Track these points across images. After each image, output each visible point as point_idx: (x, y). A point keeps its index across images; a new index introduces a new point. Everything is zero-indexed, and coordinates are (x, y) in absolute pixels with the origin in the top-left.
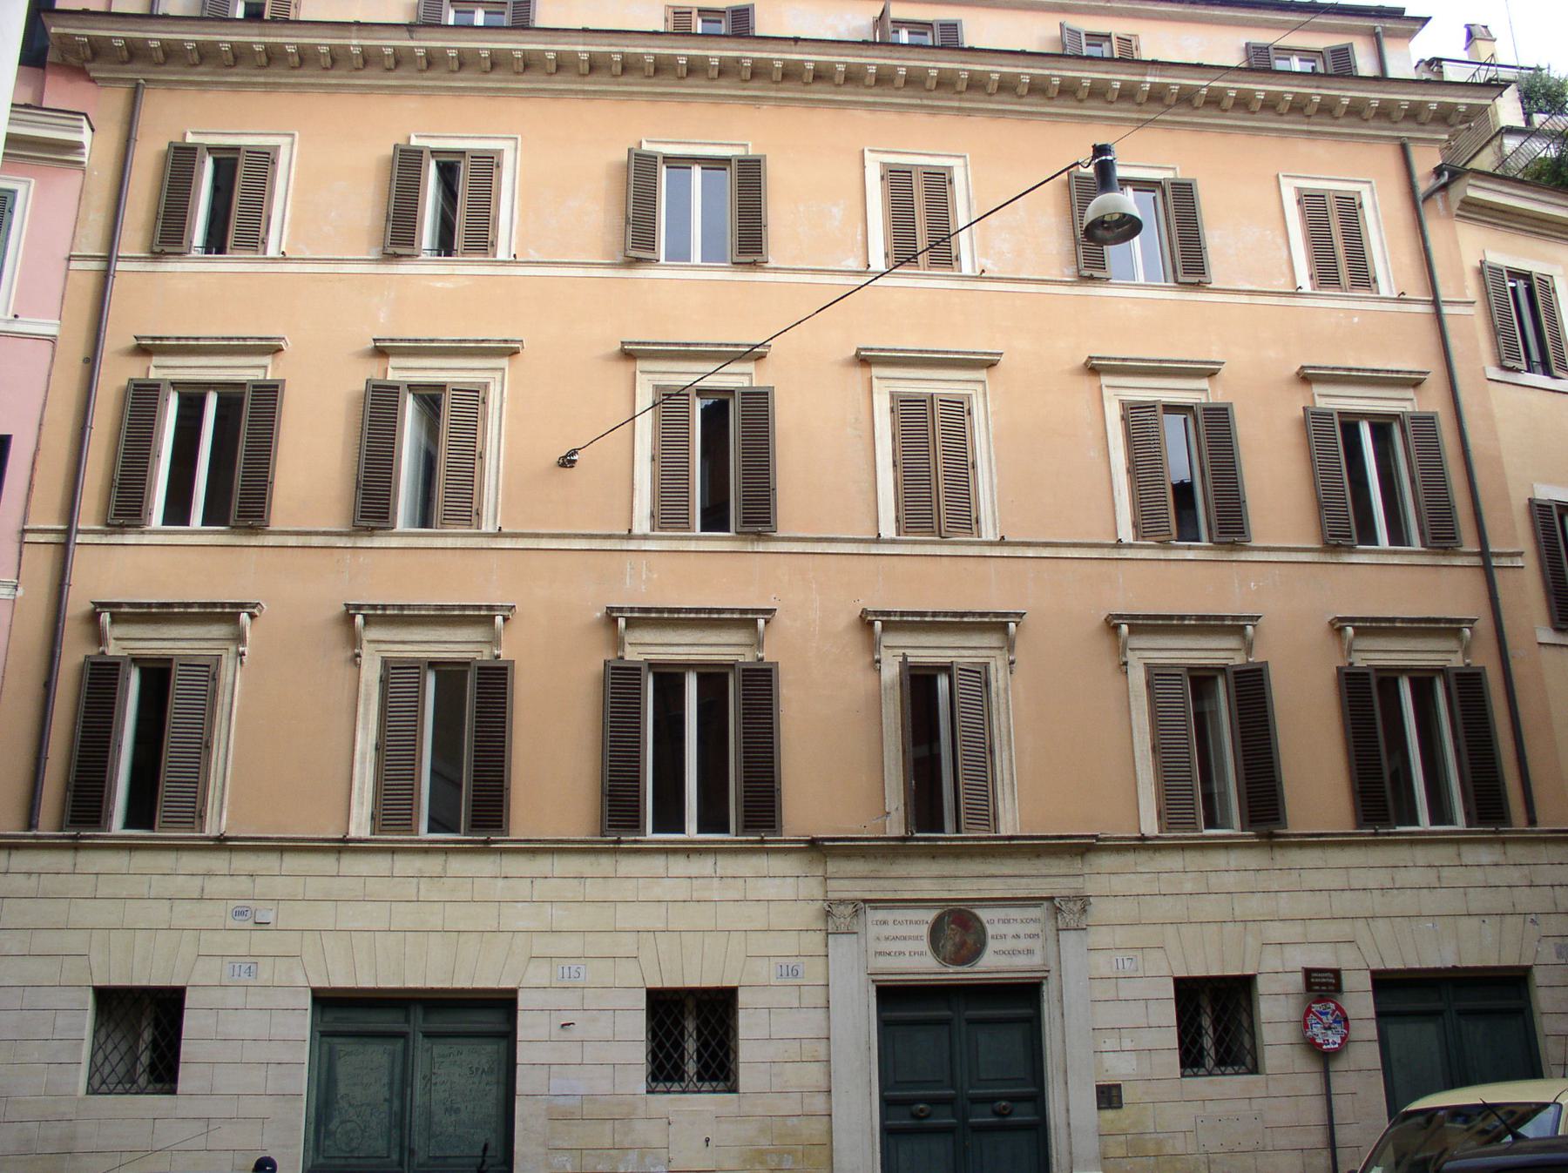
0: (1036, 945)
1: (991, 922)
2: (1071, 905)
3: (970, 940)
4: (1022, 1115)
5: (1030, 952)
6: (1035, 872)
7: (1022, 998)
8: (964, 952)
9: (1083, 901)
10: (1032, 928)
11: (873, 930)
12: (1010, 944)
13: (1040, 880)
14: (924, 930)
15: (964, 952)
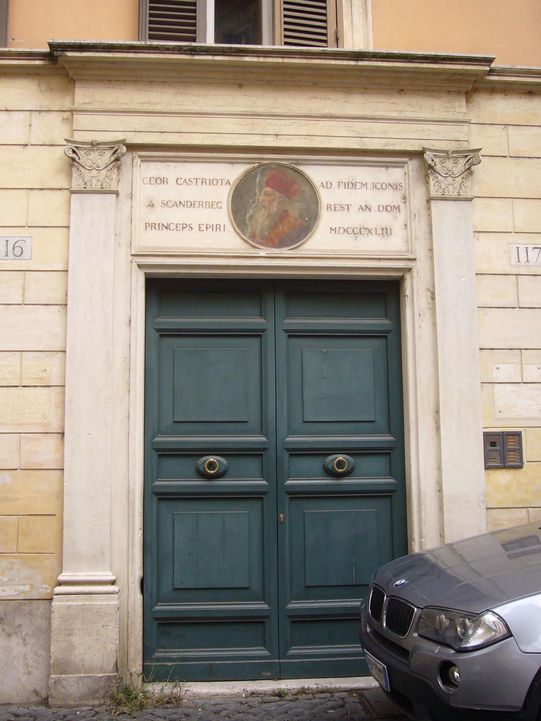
0: (396, 222)
1: (328, 185)
2: (449, 164)
3: (295, 209)
4: (370, 476)
5: (386, 232)
6: (395, 115)
7: (375, 296)
8: (284, 228)
9: (470, 157)
10: (390, 197)
11: (144, 192)
13: (401, 126)
14: (224, 194)
15: (284, 228)
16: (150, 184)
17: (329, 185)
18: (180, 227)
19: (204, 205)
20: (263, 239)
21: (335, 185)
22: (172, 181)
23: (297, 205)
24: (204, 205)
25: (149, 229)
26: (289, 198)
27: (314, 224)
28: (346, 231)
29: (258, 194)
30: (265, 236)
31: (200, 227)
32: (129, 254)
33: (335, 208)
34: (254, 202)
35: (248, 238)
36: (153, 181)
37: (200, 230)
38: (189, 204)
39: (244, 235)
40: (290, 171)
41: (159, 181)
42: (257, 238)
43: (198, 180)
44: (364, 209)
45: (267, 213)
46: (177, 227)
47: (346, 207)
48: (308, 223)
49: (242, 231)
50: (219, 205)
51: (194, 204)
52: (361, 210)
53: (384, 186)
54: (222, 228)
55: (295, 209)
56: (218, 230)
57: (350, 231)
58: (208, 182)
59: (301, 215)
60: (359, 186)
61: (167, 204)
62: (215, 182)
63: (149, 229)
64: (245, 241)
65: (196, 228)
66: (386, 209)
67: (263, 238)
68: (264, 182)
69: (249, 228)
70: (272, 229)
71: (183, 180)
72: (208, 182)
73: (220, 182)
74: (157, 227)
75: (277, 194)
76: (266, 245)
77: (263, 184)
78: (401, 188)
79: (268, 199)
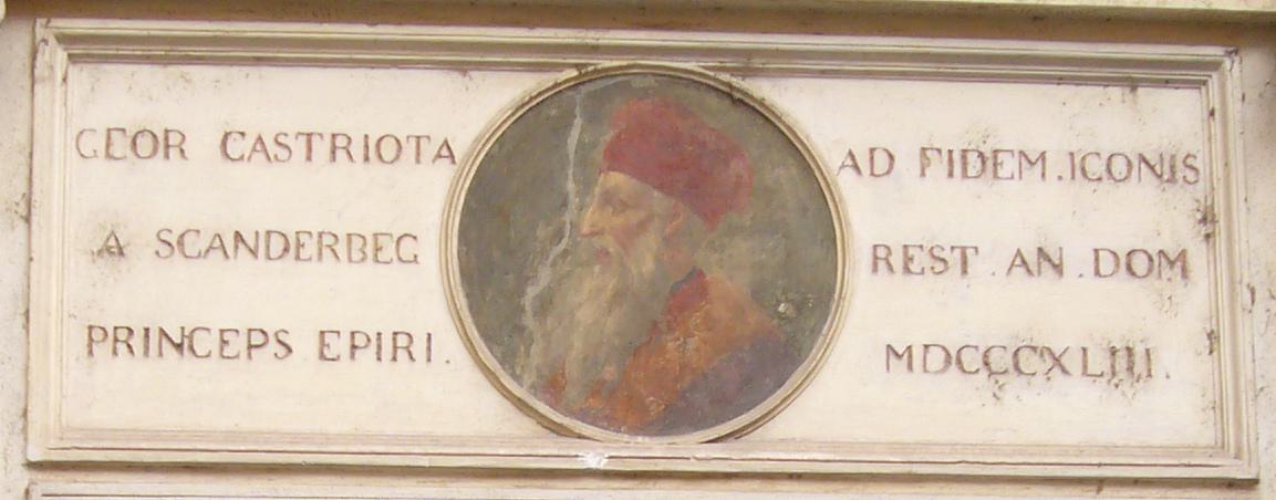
1: (877, 163)
3: (733, 266)
5: (1128, 364)
8: (687, 347)
12: (991, 309)
14: (427, 202)
15: (687, 347)
16: (109, 156)
17: (881, 162)
18: (237, 345)
19: (341, 249)
20: (595, 393)
21: (907, 163)
22: (202, 145)
23: (741, 248)
24: (341, 249)
25: (102, 350)
26: (711, 216)
27: (815, 332)
28: (954, 360)
29: (574, 200)
30: (602, 383)
31: (323, 344)
32: (18, 460)
33: (908, 260)
34: (559, 235)
35: (534, 389)
36: (121, 146)
37: (322, 357)
38: (277, 245)
39: (516, 378)
40: (713, 101)
41: (145, 144)
42: (572, 393)
43: (315, 139)
44: (1033, 268)
45: (612, 283)
46: (224, 342)
47: (954, 258)
48: (788, 328)
49: (507, 360)
50: (408, 248)
51: (300, 245)
52: (1019, 271)
53: (1119, 167)
54: (419, 349)
55: (733, 266)
56: (402, 354)
57: (972, 360)
58: (357, 150)
59: (758, 293)
60: (1009, 165)
61: (181, 242)
62: (388, 150)
63: (102, 350)
64: (520, 404)
65: (305, 347)
66: (1129, 268)
67: (596, 389)
68: (601, 148)
69: (534, 349)
70: (636, 352)
71: (250, 140)
72: (357, 150)
73: (409, 149)
74: (137, 342)
75: (658, 201)
76: (610, 421)
77: (598, 155)
78: (1191, 176)
79: (618, 221)
